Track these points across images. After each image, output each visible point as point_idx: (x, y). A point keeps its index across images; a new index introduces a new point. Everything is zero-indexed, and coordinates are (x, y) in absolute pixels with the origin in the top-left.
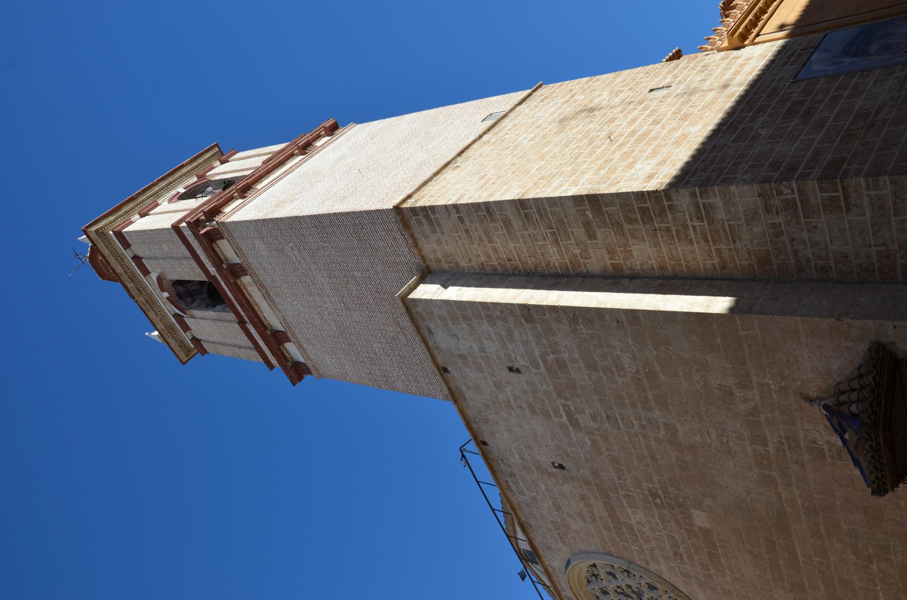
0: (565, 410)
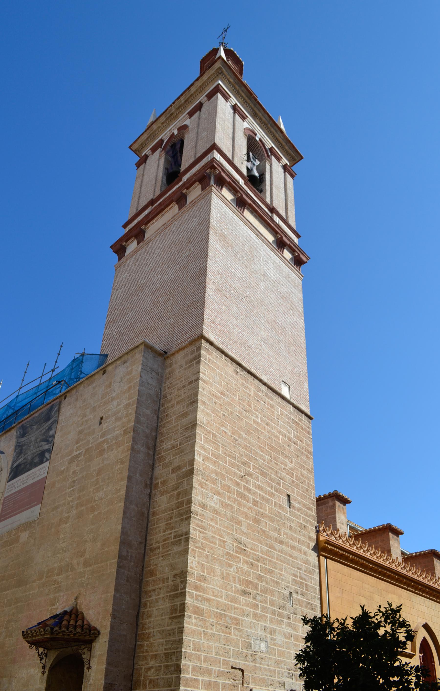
0: (79, 454)
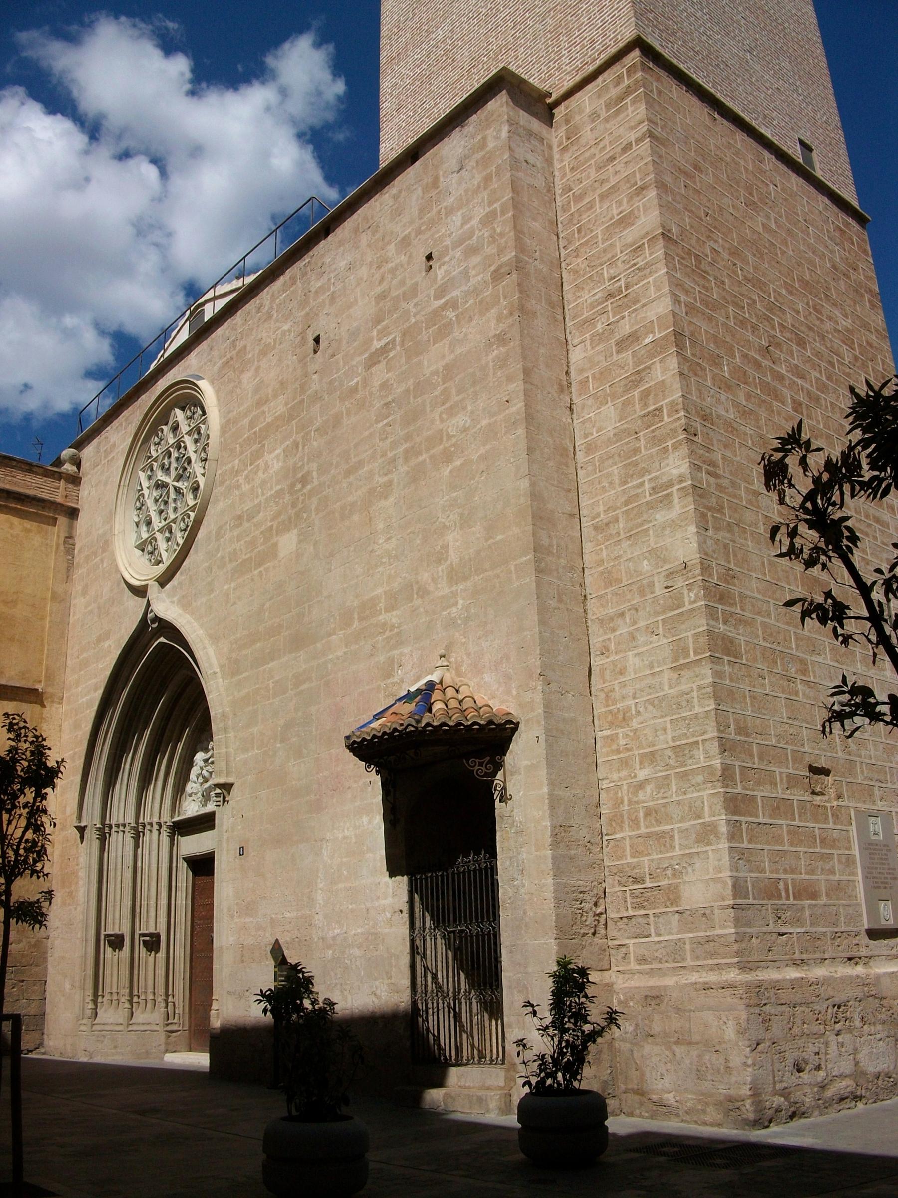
0: (388, 344)
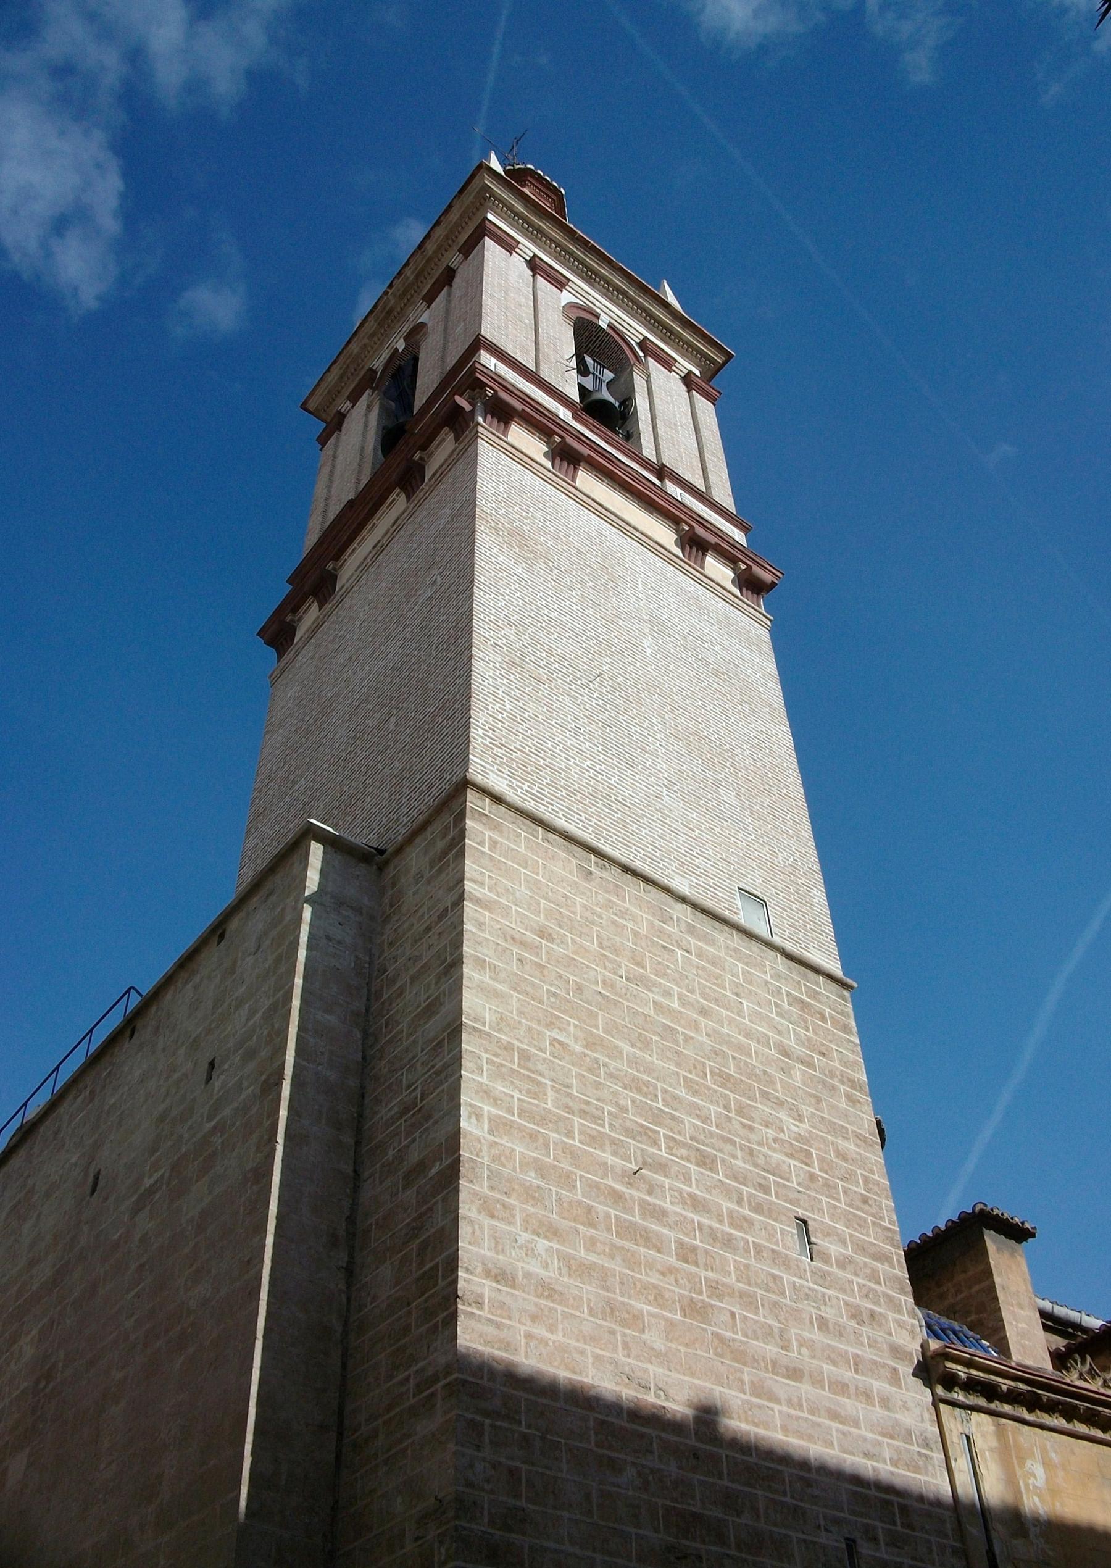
0: (156, 1182)
